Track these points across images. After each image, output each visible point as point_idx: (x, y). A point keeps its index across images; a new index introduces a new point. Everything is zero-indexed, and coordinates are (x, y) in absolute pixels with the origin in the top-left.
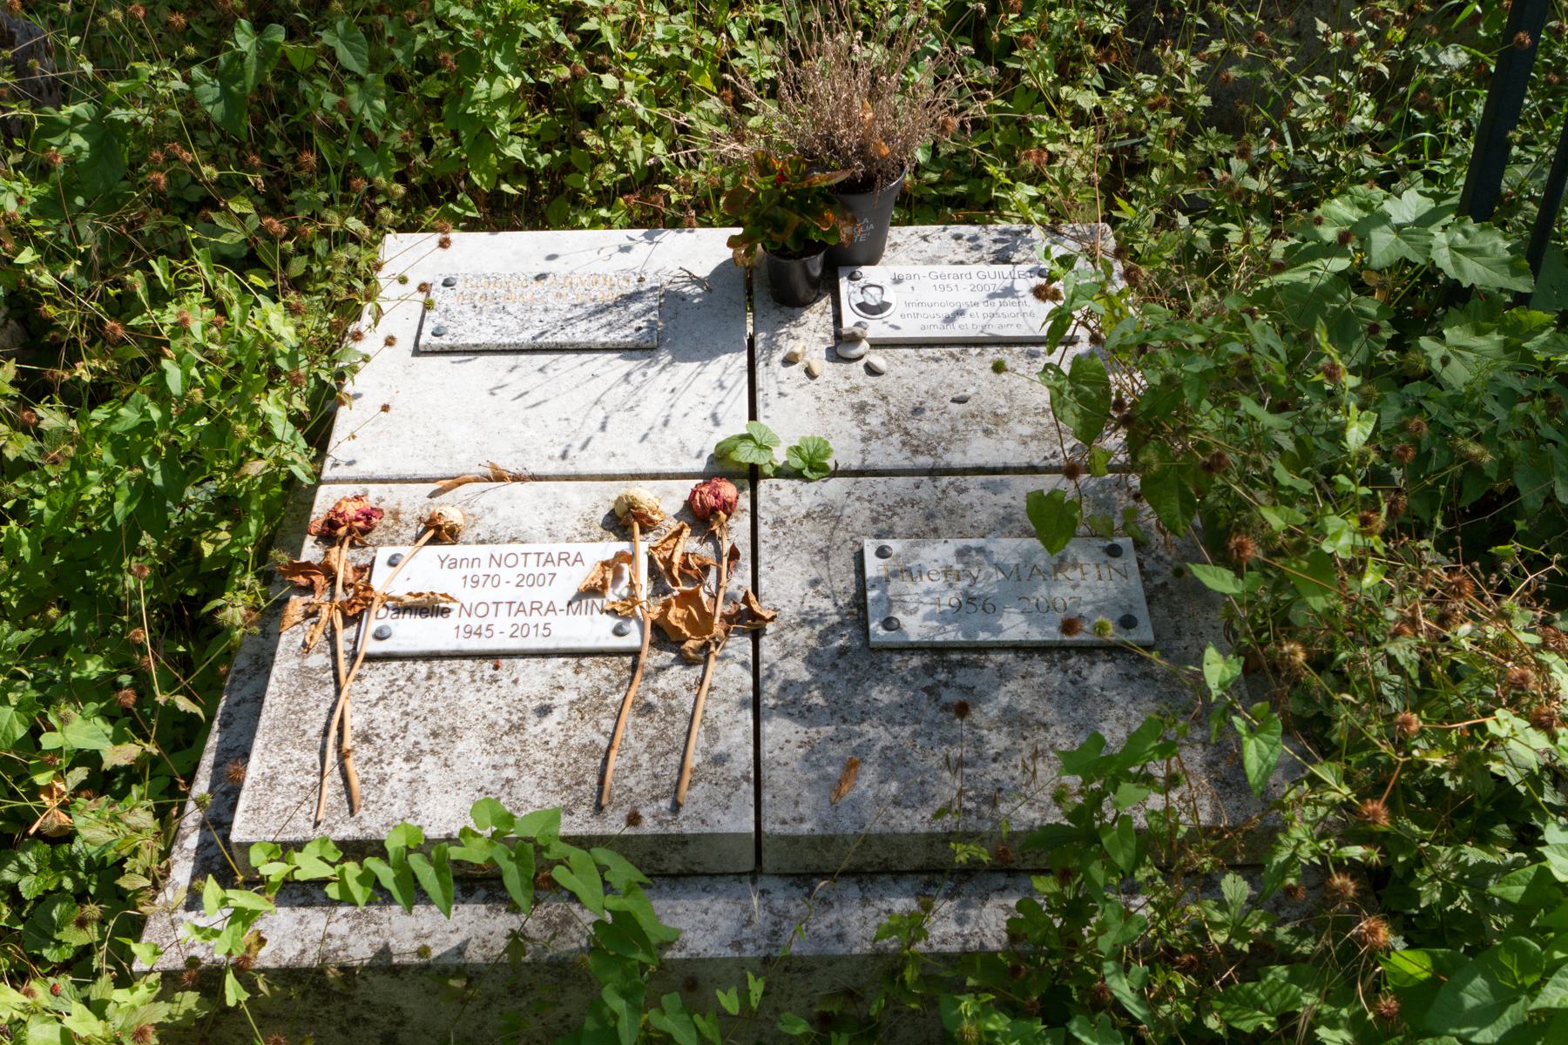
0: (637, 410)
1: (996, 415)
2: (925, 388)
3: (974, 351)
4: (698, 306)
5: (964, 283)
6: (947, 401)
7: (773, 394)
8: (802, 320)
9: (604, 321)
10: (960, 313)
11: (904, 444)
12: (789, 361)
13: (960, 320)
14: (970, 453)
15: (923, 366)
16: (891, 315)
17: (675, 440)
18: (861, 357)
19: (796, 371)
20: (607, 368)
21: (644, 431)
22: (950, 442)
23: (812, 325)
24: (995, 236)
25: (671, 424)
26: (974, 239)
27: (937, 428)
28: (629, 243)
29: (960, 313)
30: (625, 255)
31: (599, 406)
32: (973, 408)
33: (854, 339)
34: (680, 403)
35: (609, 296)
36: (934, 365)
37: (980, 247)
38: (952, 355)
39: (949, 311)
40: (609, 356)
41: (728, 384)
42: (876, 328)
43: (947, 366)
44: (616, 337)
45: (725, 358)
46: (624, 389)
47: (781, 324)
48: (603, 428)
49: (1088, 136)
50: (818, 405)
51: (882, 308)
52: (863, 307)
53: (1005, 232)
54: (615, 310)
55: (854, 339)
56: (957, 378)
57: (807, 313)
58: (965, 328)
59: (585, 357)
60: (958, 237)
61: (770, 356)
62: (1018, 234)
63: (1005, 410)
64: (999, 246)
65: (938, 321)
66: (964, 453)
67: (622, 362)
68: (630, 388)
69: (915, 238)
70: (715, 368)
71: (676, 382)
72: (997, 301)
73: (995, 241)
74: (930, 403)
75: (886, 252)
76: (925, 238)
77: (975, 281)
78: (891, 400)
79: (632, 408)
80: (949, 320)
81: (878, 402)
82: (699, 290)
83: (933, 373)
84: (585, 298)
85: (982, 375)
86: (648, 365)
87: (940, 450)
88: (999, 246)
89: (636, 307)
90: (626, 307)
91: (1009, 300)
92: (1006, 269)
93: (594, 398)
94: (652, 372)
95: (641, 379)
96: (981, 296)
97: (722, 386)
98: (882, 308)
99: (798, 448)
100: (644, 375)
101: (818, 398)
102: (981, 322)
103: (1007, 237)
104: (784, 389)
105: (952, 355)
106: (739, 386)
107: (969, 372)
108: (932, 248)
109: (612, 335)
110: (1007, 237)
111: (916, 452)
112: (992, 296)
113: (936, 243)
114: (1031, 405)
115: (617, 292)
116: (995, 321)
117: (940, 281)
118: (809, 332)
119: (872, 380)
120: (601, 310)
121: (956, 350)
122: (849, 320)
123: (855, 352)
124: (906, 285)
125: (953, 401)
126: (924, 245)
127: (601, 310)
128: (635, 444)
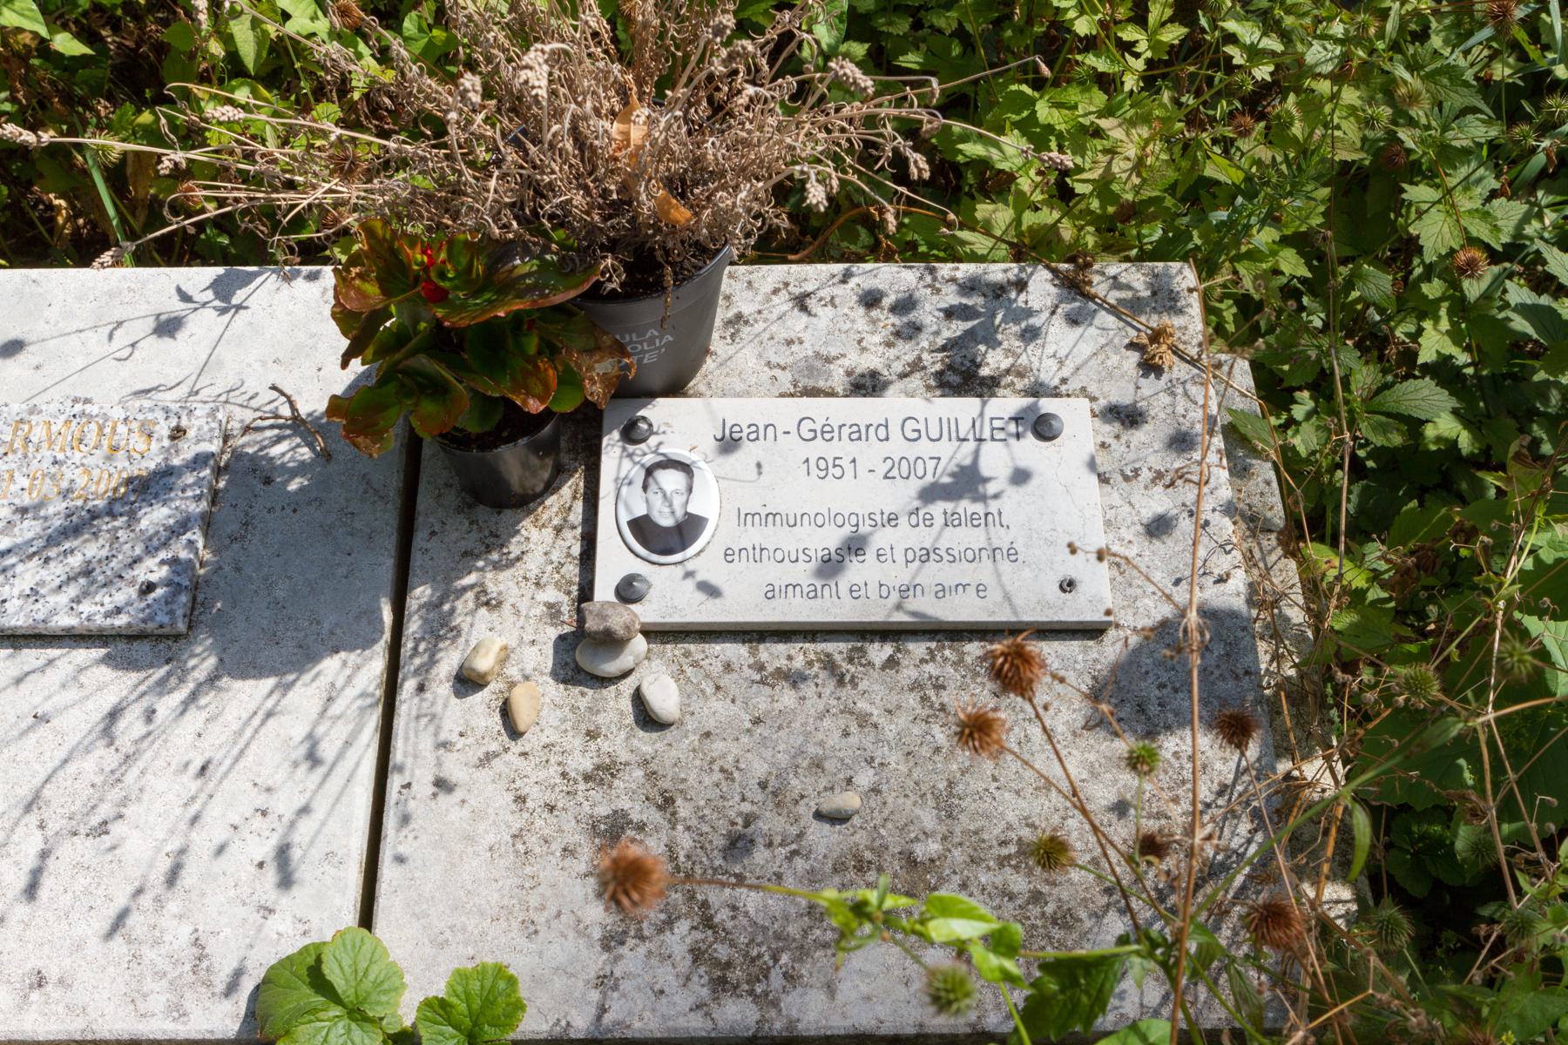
0: (117, 829)
1: (911, 862)
2: (759, 769)
3: (879, 652)
4: (294, 504)
5: (872, 453)
6: (805, 811)
7: (423, 787)
8: (514, 549)
9: (75, 561)
10: (855, 546)
11: (697, 954)
12: (467, 682)
13: (857, 571)
14: (848, 990)
15: (762, 700)
16: (703, 556)
17: (185, 931)
18: (626, 674)
19: (480, 708)
20: (72, 694)
21: (121, 901)
22: (802, 953)
23: (532, 564)
24: (951, 297)
25: (188, 878)
26: (905, 305)
27: (775, 904)
28: (177, 306)
29: (855, 546)
30: (166, 342)
31: (33, 819)
32: (861, 838)
33: (611, 642)
34: (213, 812)
35: (97, 478)
36: (787, 697)
37: (917, 328)
38: (829, 664)
39: (831, 539)
40: (83, 655)
41: (328, 750)
42: (670, 594)
43: (819, 695)
44: (95, 611)
45: (331, 666)
46: (106, 758)
47: (467, 558)
48: (31, 890)
49: (1195, 294)
50: (517, 823)
51: (686, 530)
52: (642, 528)
53: (970, 287)
54: (105, 525)
55: (611, 642)
56: (834, 739)
57: (527, 527)
58: (863, 594)
59: (32, 657)
60: (871, 300)
61: (432, 662)
62: (998, 292)
63: (934, 847)
64: (958, 327)
65: (802, 573)
66: (831, 989)
67: (105, 673)
68: (111, 759)
69: (782, 303)
70: (306, 694)
71: (216, 742)
72: (938, 509)
73: (950, 313)
74: (771, 823)
75: (717, 343)
76: (801, 302)
77: (897, 447)
78: (684, 809)
79: (103, 829)
80: (830, 567)
81: (653, 816)
82: (305, 453)
83: (784, 720)
84: (48, 488)
85: (890, 729)
86: (162, 687)
87: (776, 980)
88: (958, 327)
89: (155, 517)
90: (133, 517)
91: (966, 506)
92: (964, 408)
93: (25, 792)
94: (167, 705)
95: (139, 729)
96: (903, 494)
97: (313, 759)
98: (686, 530)
99: (443, 1004)
100: (150, 715)
101: (521, 799)
102: (898, 574)
103: (976, 301)
104: (454, 769)
105: (829, 664)
106: (352, 755)
107: (864, 720)
108: (814, 331)
109: (86, 607)
110: (976, 301)
111: (721, 985)
112: (931, 494)
113: (824, 314)
114: (994, 832)
115: (125, 468)
116: (932, 574)
117: (819, 448)
118: (509, 612)
119: (646, 742)
120: (79, 525)
121: (838, 649)
122: (616, 559)
123: (611, 667)
124: (748, 453)
125: (819, 816)
126: (798, 321)
127: (79, 525)
128: (94, 946)
